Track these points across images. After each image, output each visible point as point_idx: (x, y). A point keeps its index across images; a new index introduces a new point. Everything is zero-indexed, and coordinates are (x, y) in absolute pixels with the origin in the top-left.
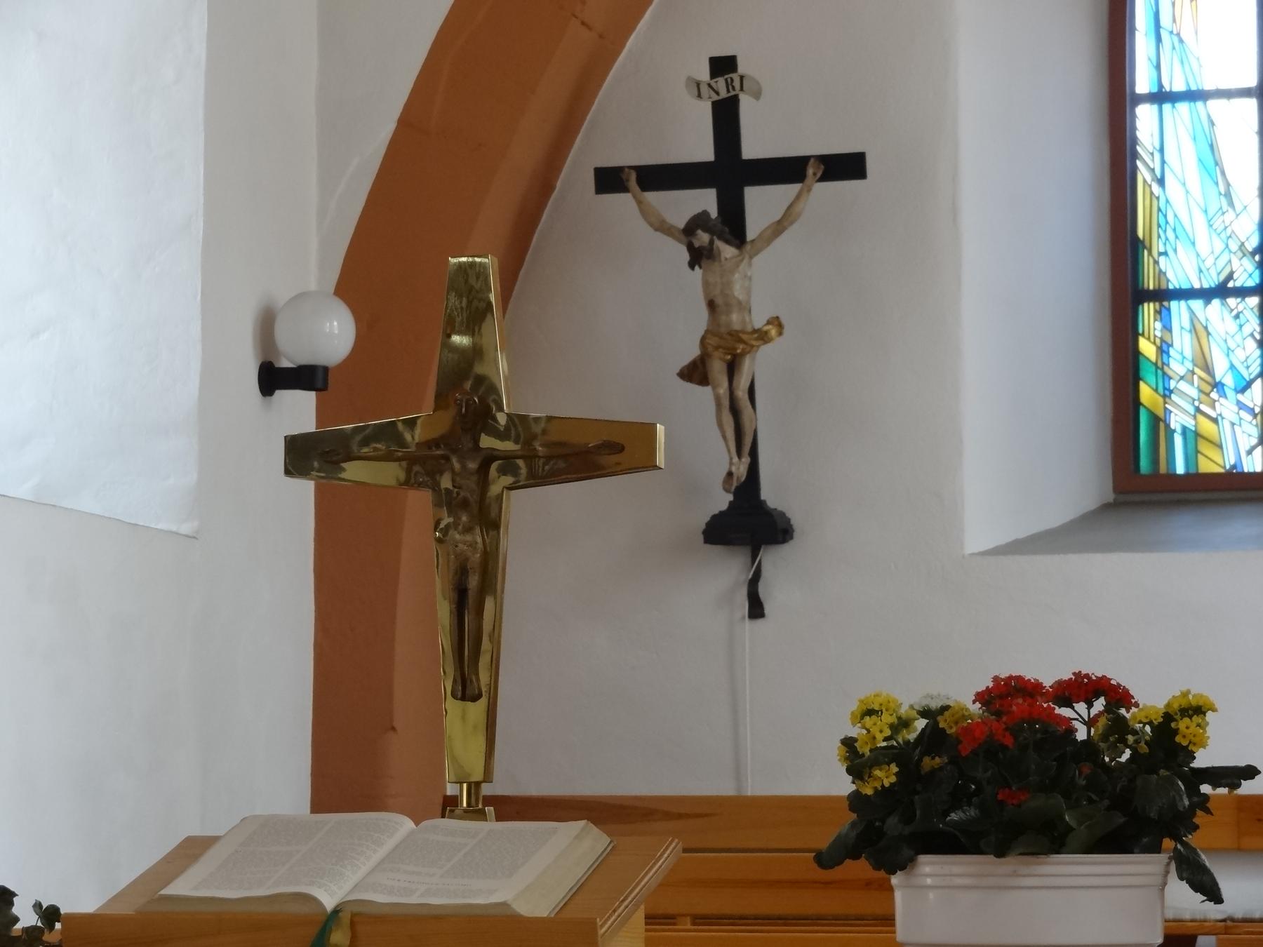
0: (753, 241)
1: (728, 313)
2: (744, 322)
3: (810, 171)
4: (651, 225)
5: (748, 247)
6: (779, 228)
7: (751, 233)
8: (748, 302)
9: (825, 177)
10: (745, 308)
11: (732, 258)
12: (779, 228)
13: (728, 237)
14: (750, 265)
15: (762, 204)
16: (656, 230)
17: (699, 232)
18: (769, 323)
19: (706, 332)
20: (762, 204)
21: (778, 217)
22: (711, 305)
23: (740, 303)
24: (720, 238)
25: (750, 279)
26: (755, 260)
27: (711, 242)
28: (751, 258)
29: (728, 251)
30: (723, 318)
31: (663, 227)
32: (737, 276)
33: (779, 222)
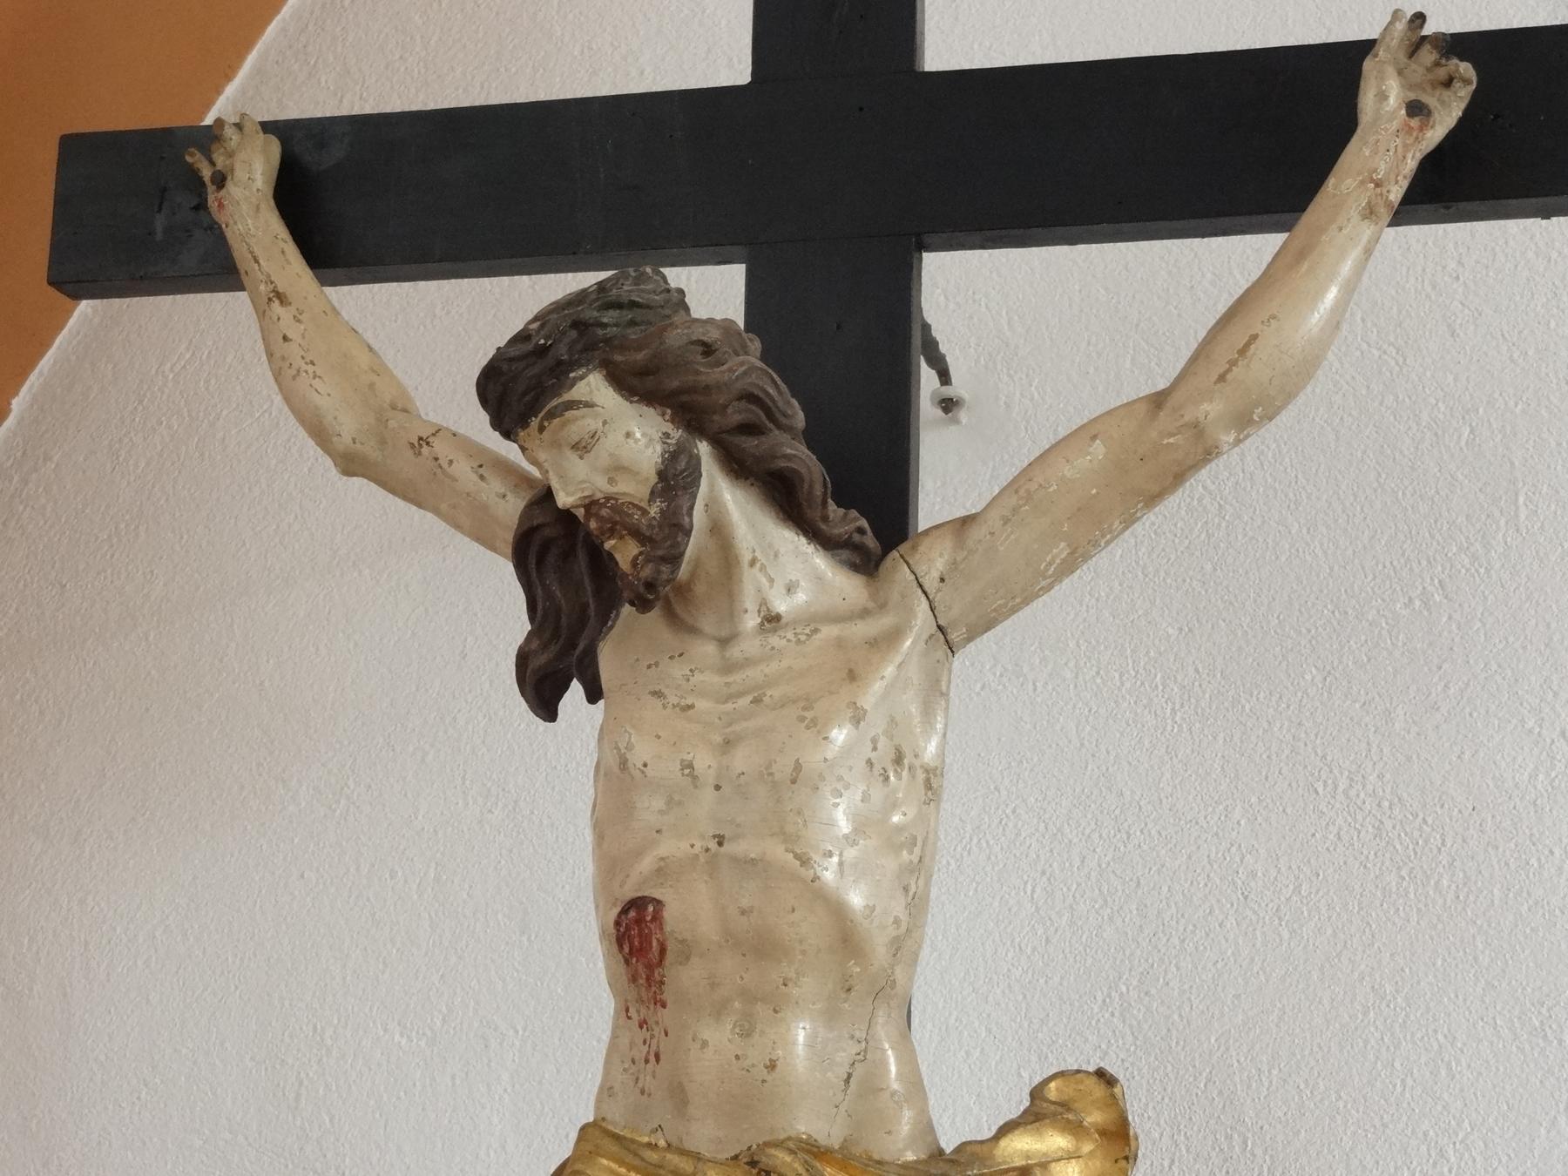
0: (965, 523)
1: (759, 1006)
2: (861, 1081)
3: (1383, 95)
4: (320, 434)
5: (932, 560)
6: (1159, 447)
7: (950, 474)
8: (905, 945)
9: (1451, 184)
10: (865, 974)
11: (812, 621)
12: (1159, 447)
13: (798, 455)
14: (934, 691)
15: (1025, 333)
16: (350, 464)
17: (593, 386)
18: (1038, 1112)
19: (594, 1137)
20: (1025, 333)
21: (1162, 385)
22: (637, 936)
23: (846, 938)
24: (738, 467)
25: (931, 782)
26: (976, 662)
27: (675, 480)
28: (946, 638)
29: (786, 570)
30: (711, 1047)
31: (385, 456)
32: (840, 735)
33: (1158, 401)
